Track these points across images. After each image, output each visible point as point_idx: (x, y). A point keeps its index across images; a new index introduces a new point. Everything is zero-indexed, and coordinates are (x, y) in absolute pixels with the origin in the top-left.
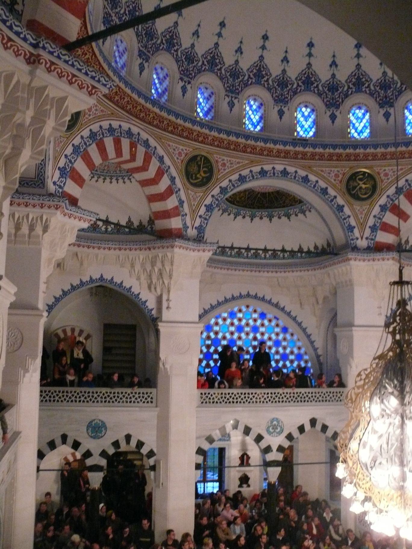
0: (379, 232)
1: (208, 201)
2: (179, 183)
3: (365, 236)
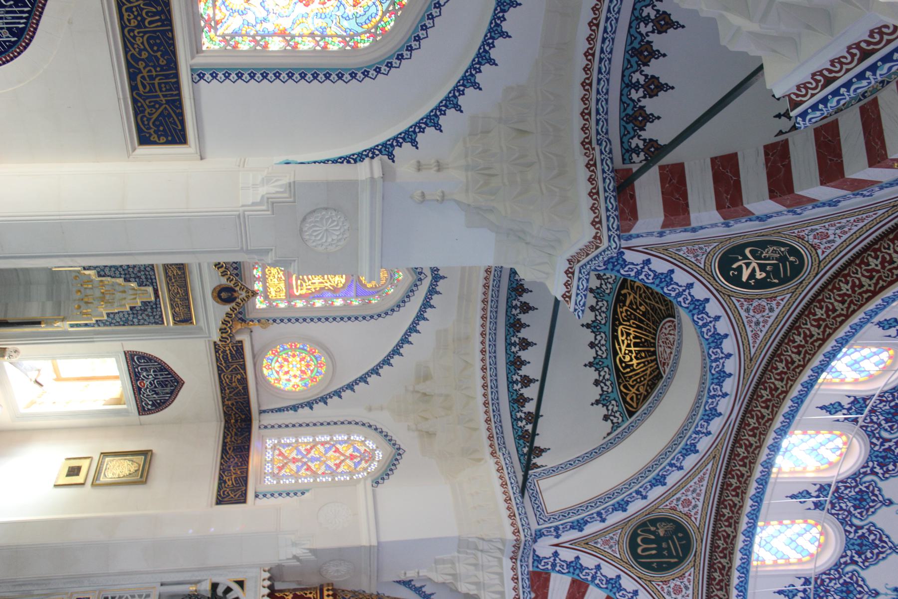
0: (566, 580)
1: (681, 277)
3: (559, 549)
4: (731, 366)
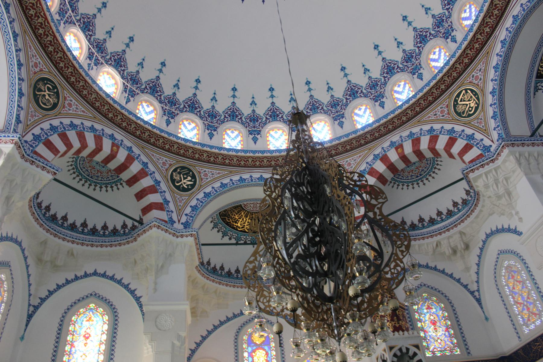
2: (163, 186)
4: (236, 178)
